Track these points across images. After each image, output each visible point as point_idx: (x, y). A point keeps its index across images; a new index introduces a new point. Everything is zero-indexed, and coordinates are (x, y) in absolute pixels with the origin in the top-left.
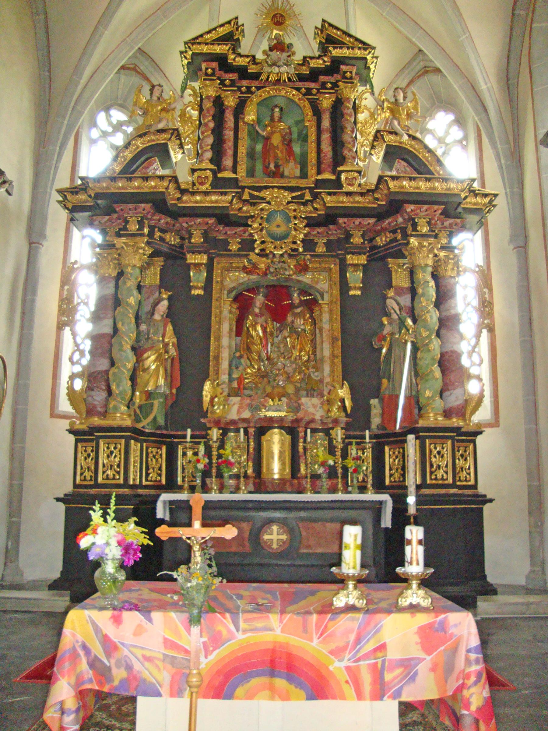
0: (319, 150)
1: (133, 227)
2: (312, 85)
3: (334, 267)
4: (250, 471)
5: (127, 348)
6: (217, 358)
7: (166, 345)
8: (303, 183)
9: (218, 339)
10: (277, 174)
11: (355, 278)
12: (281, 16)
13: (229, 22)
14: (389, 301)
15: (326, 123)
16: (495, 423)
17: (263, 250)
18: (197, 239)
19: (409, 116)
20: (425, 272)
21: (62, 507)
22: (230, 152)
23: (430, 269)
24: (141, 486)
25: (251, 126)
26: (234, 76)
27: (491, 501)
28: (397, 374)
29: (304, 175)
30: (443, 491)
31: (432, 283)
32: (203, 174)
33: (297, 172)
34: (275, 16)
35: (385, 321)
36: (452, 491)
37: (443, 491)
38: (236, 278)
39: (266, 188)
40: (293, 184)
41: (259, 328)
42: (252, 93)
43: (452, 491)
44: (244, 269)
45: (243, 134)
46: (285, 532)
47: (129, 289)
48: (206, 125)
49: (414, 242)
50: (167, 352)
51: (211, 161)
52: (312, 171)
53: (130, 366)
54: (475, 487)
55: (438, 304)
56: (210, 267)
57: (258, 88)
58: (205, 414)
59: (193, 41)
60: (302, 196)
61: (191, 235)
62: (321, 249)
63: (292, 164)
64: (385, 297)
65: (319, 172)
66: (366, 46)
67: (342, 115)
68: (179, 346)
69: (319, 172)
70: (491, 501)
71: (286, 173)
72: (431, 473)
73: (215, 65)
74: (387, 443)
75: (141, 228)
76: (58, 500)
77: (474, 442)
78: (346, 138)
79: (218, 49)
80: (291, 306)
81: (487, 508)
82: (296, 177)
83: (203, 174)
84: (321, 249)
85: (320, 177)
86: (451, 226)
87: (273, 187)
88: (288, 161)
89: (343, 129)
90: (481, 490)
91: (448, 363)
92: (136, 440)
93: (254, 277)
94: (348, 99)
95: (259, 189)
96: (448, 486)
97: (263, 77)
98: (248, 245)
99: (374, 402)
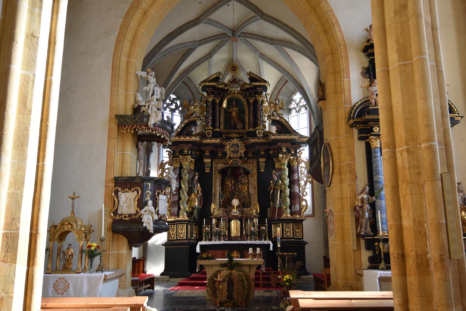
0: (249, 119)
1: (186, 152)
2: (247, 93)
3: (255, 162)
4: (227, 234)
5: (186, 193)
6: (215, 195)
7: (198, 191)
8: (243, 131)
9: (215, 188)
10: (235, 127)
11: (262, 165)
12: (235, 67)
13: (216, 74)
14: (273, 175)
15: (252, 109)
16: (313, 215)
17: (230, 157)
18: (207, 154)
19: (280, 108)
20: (284, 165)
21: (164, 246)
22: (218, 121)
23: (286, 165)
24: (177, 240)
25: (225, 109)
26: (218, 91)
27: (307, 243)
28: (276, 201)
29: (244, 128)
30: (289, 240)
31: (287, 169)
32: (209, 131)
33: (242, 127)
34: (233, 67)
35: (271, 182)
36: (292, 240)
37: (289, 240)
38: (220, 166)
39: (231, 133)
40: (240, 131)
41: (229, 182)
42: (225, 96)
43: (292, 240)
44: (224, 163)
45: (222, 113)
46: (238, 253)
47: (185, 174)
48: (209, 112)
49: (281, 155)
50: (198, 194)
51: (211, 126)
52: (247, 127)
53: (186, 199)
54: (302, 238)
55: (289, 177)
56: (212, 162)
57: (227, 94)
58: (212, 215)
59: (204, 81)
60: (244, 136)
61: (205, 153)
62: (250, 155)
63: (240, 124)
64: (272, 173)
65: (249, 128)
66: (265, 81)
67: (257, 107)
68: (202, 191)
69: (249, 128)
70: (307, 243)
71: (238, 127)
72: (285, 234)
73: (212, 89)
74: (273, 224)
75: (188, 152)
76: (163, 245)
77: (302, 223)
78: (259, 116)
79: (212, 84)
80: (240, 174)
81: (306, 246)
82: (241, 129)
83: (209, 131)
84: (250, 155)
85: (249, 130)
86: (295, 147)
87: (233, 133)
88: (238, 122)
89: (257, 112)
90: (304, 240)
91: (293, 196)
92: (189, 224)
93: (227, 166)
94: (259, 101)
95: (229, 134)
96: (291, 238)
97: (229, 92)
98: (225, 154)
99: (269, 209)
